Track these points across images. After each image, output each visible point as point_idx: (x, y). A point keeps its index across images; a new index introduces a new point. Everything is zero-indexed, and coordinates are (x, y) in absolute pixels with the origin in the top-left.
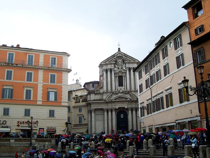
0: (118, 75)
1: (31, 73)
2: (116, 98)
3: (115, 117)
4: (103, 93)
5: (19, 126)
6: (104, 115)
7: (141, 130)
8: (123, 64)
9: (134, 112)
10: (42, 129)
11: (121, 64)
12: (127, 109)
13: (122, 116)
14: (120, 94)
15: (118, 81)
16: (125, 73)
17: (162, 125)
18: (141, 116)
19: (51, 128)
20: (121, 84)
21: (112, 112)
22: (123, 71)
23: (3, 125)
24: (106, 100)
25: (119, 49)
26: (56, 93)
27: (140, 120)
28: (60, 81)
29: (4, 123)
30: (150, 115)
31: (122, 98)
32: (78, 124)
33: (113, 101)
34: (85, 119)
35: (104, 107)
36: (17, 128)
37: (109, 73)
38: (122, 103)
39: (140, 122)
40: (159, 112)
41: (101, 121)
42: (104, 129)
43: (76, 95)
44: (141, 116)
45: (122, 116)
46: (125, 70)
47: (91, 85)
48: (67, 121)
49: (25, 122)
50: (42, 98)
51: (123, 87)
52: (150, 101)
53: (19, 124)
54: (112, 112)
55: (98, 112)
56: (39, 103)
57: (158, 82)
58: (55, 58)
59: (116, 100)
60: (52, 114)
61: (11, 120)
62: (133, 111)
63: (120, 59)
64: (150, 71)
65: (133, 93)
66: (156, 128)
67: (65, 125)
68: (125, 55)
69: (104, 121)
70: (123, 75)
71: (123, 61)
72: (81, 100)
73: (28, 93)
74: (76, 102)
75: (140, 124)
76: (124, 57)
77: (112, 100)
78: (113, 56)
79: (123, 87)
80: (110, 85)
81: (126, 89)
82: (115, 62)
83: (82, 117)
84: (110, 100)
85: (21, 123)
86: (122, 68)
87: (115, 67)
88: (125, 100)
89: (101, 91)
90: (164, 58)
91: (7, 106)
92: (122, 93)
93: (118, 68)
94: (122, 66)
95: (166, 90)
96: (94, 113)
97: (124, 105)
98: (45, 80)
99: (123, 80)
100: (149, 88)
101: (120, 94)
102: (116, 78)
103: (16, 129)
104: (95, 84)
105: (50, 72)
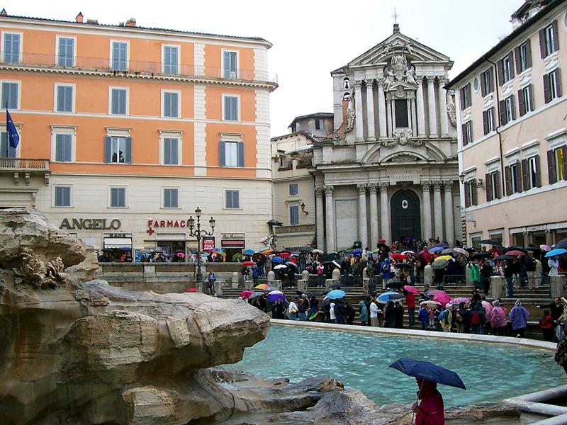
0: (395, 96)
1: (175, 95)
2: (390, 157)
4: (356, 144)
5: (153, 232)
7: (466, 241)
8: (407, 69)
9: (448, 195)
10: (209, 238)
11: (401, 68)
12: (420, 187)
13: (405, 205)
14: (400, 149)
15: (394, 113)
17: (532, 228)
18: (467, 205)
19: (231, 237)
20: (402, 121)
21: (379, 194)
22: (409, 87)
23: (112, 231)
24: (364, 164)
25: (396, 25)
26: (241, 147)
27: (463, 215)
28: (251, 114)
29: (116, 225)
30: (495, 201)
31: (406, 159)
32: (289, 225)
33: (382, 164)
34: (307, 213)
35: (360, 180)
36: (148, 237)
37: (370, 91)
38: (405, 170)
39: (462, 219)
40: (524, 194)
41: (349, 217)
43: (279, 151)
44: (467, 205)
45: (405, 204)
46: (412, 84)
47: (312, 122)
48: (270, 219)
49: (166, 222)
50: (207, 158)
52: (497, 167)
53: (151, 228)
54: (379, 194)
55: (342, 195)
56: (199, 172)
57: (525, 116)
58: (234, 54)
59: (391, 164)
60: (232, 200)
61: (132, 217)
63: (400, 54)
64: (499, 87)
65: (435, 144)
66: (513, 234)
67: (267, 229)
68: (413, 43)
69: (358, 216)
71: (409, 59)
72: (295, 163)
73: (171, 146)
74: (279, 170)
75: (464, 226)
76: (412, 48)
77: (380, 163)
78: (382, 45)
79: (409, 129)
82: (386, 63)
83: (300, 208)
84: (376, 163)
85: (156, 225)
86: (404, 79)
87: (386, 76)
88: (415, 163)
89: (350, 139)
90: (545, 54)
91: (232, 186)
92: (405, 144)
93: (395, 79)
94: (405, 72)
95: (550, 140)
96: (331, 197)
98: (211, 112)
99: (409, 111)
100: (492, 133)
101: (400, 149)
102: (389, 106)
103: (145, 241)
104: (321, 122)
105: (224, 92)
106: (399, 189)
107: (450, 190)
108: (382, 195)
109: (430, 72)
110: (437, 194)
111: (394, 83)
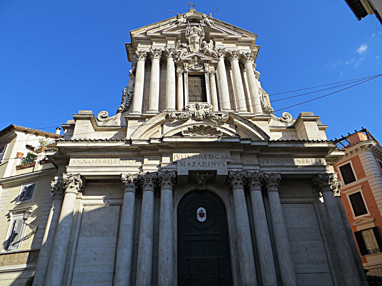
3: (172, 213)
6: (121, 209)
8: (205, 42)
11: (197, 40)
22: (206, 58)
41: (103, 234)
42: (114, 273)
51: (207, 105)
62: (250, 195)
97: (210, 161)
102: (180, 79)
106: (192, 188)
107: (276, 189)
108: (163, 192)
109: (230, 47)
110: (257, 194)
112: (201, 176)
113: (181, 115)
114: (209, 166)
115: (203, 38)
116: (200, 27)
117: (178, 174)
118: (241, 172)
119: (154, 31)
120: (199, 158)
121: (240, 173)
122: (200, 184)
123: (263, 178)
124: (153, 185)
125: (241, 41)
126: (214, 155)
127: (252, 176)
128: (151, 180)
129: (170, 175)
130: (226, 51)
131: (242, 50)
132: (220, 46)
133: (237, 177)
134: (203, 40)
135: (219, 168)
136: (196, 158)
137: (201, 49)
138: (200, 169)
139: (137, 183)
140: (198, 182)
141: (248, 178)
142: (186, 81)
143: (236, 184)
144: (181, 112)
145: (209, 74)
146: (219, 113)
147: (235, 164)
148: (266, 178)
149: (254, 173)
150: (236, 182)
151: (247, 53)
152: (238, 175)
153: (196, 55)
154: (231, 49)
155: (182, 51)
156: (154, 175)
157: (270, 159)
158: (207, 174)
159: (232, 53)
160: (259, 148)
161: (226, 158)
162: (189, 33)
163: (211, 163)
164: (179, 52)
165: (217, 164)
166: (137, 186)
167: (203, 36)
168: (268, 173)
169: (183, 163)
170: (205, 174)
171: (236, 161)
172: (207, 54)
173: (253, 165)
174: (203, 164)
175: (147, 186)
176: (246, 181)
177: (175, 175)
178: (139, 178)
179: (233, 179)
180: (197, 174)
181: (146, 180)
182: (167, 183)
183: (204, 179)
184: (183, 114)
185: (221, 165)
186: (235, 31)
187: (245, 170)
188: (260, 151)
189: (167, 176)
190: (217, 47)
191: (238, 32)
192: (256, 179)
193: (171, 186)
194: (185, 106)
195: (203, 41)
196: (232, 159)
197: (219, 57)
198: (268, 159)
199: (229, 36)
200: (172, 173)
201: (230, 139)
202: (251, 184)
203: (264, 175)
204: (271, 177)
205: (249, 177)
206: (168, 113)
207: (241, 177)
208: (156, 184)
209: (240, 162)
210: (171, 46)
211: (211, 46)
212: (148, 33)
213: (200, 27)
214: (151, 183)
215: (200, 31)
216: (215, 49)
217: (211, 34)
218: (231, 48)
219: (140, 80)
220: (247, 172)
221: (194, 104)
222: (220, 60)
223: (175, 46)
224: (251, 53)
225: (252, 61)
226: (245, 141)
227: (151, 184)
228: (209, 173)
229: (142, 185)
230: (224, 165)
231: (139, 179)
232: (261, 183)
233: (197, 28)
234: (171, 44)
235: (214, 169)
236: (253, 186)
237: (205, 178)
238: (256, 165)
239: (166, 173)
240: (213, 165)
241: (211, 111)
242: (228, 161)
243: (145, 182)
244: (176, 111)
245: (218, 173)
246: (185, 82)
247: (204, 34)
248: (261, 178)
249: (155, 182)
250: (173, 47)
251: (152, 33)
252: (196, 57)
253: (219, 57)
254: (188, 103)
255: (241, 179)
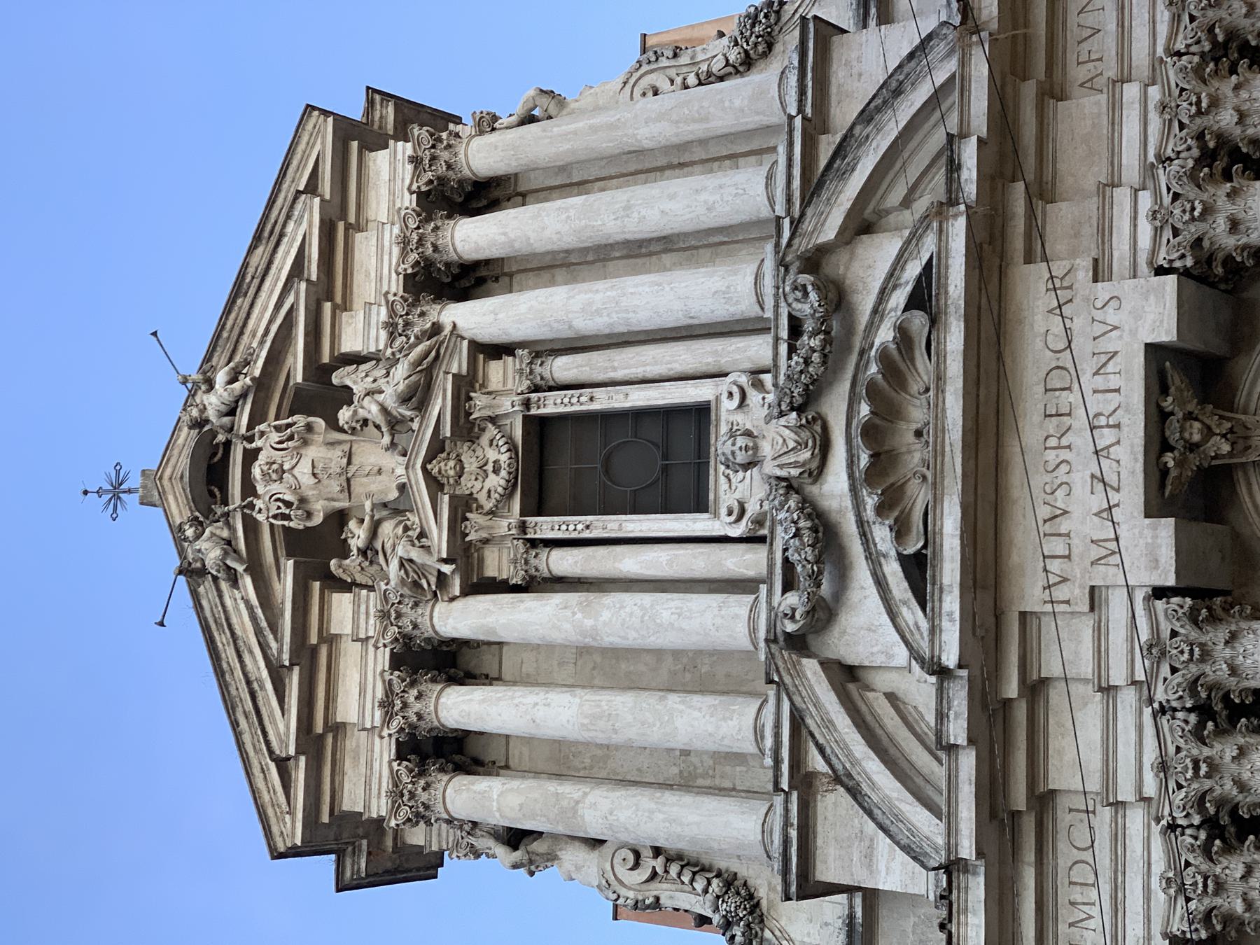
8: (344, 415)
11: (335, 458)
16: (497, 373)
22: (441, 403)
51: (728, 405)
70: (507, 405)
80: (673, 699)
81: (758, 349)
99: (605, 401)
102: (563, 562)
111: (413, 518)
112: (1182, 438)
113: (796, 557)
114: (1118, 391)
115: (319, 423)
116: (258, 443)
117: (1171, 581)
118: (1157, 194)
119: (272, 715)
120: (1065, 455)
121: (1167, 200)
122: (1233, 444)
123: (1196, 59)
124: (1241, 741)
125: (337, 200)
126: (1049, 359)
127: (1182, 126)
128: (1206, 752)
129: (1174, 634)
130: (401, 293)
131: (392, 193)
132: (367, 323)
133: (1193, 219)
134: (333, 424)
135: (1134, 333)
136: (1064, 468)
137: (386, 440)
138: (1140, 449)
139: (1224, 840)
140: (1216, 457)
141: (1196, 152)
142: (574, 525)
143: (1234, 225)
144: (771, 566)
145: (537, 389)
146: (784, 334)
147: (1104, 231)
148: (1198, 42)
149: (1167, 117)
150: (1221, 224)
151: (409, 168)
152: (1177, 212)
153: (424, 468)
154: (386, 258)
155: (400, 551)
156: (1172, 730)
157: (1073, 19)
158: (1168, 403)
159: (413, 257)
160: (1009, 89)
161: (1070, 287)
162: (288, 504)
163: (1099, 382)
164: (402, 565)
165: (1108, 345)
166: (1242, 840)
167: (309, 428)
168: (1163, 30)
169: (1096, 552)
170: (1172, 413)
171: (1089, 230)
172: (418, 396)
173: (1115, 123)
174: (1106, 431)
175: (1246, 775)
176: (1219, 165)
177: (1175, 600)
178: (1191, 826)
179: (1206, 244)
180: (1171, 464)
181: (1208, 784)
182: (1228, 653)
183: (1203, 423)
184: (785, 550)
185: (1112, 317)
186: (282, 235)
187: (1149, 171)
188: (1024, 79)
189: (1182, 652)
190: (377, 340)
191: (288, 217)
192: (1204, 105)
193: (1244, 625)
194: (735, 532)
195: (341, 422)
196: (1074, 253)
197: (436, 329)
198: (1073, 32)
199: (313, 271)
200: (1161, 618)
201: (947, 267)
202: (1238, 131)
203: (1179, 54)
204: (1195, 13)
205: (1189, 149)
206: (781, 639)
207: (1192, 196)
208: (1233, 722)
209: (1093, 204)
210: (363, 617)
211: (370, 379)
212: (287, 746)
213: (258, 443)
214: (1225, 750)
215: (280, 442)
216: (389, 351)
217: (299, 379)
218: (380, 259)
219: (565, 803)
220: (1164, 160)
221: (722, 480)
222: (455, 326)
223: (364, 592)
224: (409, 145)
225: (457, 135)
226: (965, 175)
227: (1230, 752)
228: (1165, 390)
229: (1236, 807)
230: (1114, 303)
231: (1198, 828)
232: (1233, 70)
233: (262, 458)
234: (356, 613)
235: (1140, 359)
236: (1249, 121)
237: (1196, 419)
238: (1116, 106)
239: (1163, 653)
240: (1110, 367)
241: (767, 378)
242: (1083, 274)
243: (1218, 791)
244: (763, 588)
245: (1167, 333)
246: (587, 535)
247: (300, 420)
248: (1198, 71)
249: (1216, 726)
250: (372, 603)
251: (288, 727)
252: (434, 467)
253: (436, 329)
254: (716, 515)
255: (1205, 197)
